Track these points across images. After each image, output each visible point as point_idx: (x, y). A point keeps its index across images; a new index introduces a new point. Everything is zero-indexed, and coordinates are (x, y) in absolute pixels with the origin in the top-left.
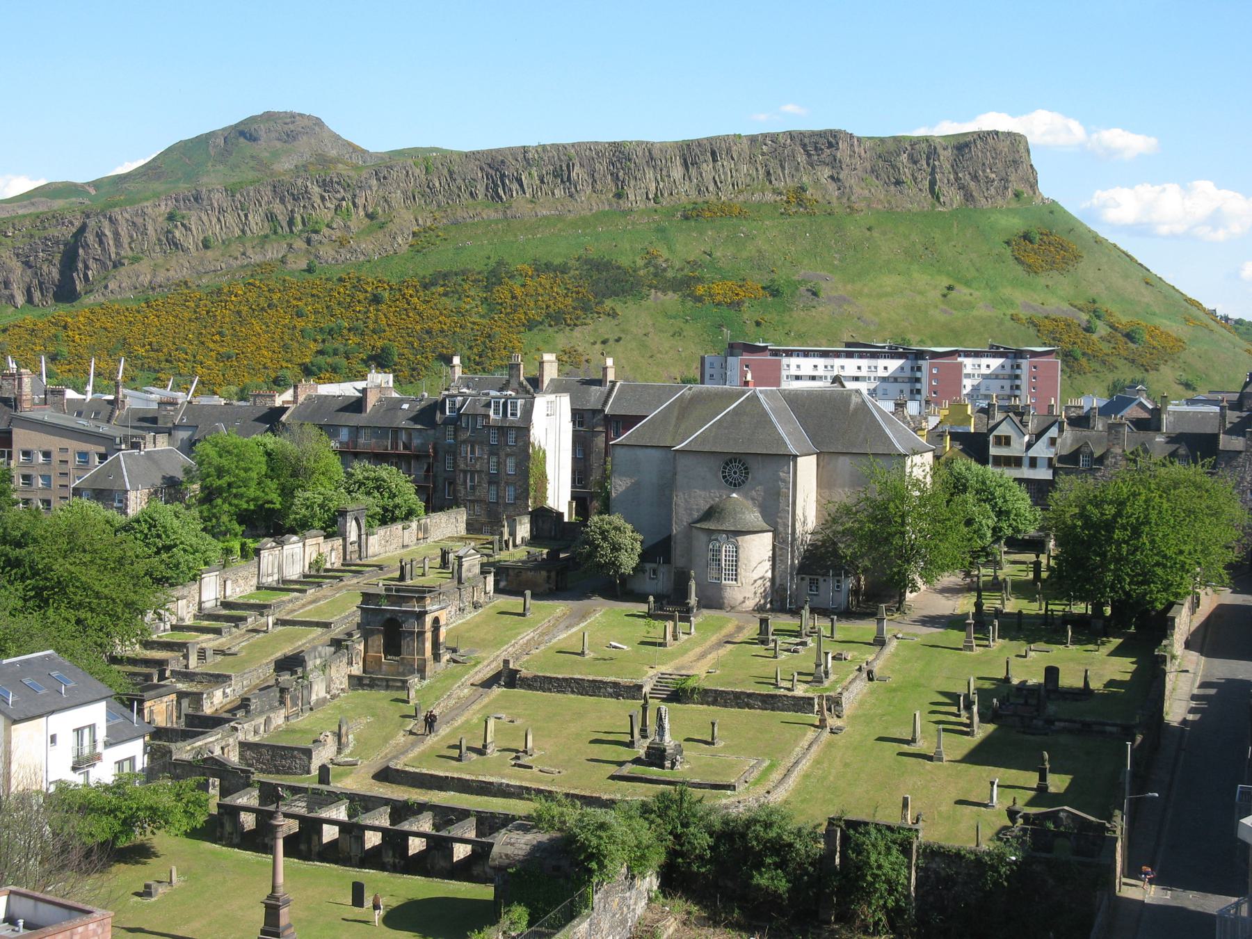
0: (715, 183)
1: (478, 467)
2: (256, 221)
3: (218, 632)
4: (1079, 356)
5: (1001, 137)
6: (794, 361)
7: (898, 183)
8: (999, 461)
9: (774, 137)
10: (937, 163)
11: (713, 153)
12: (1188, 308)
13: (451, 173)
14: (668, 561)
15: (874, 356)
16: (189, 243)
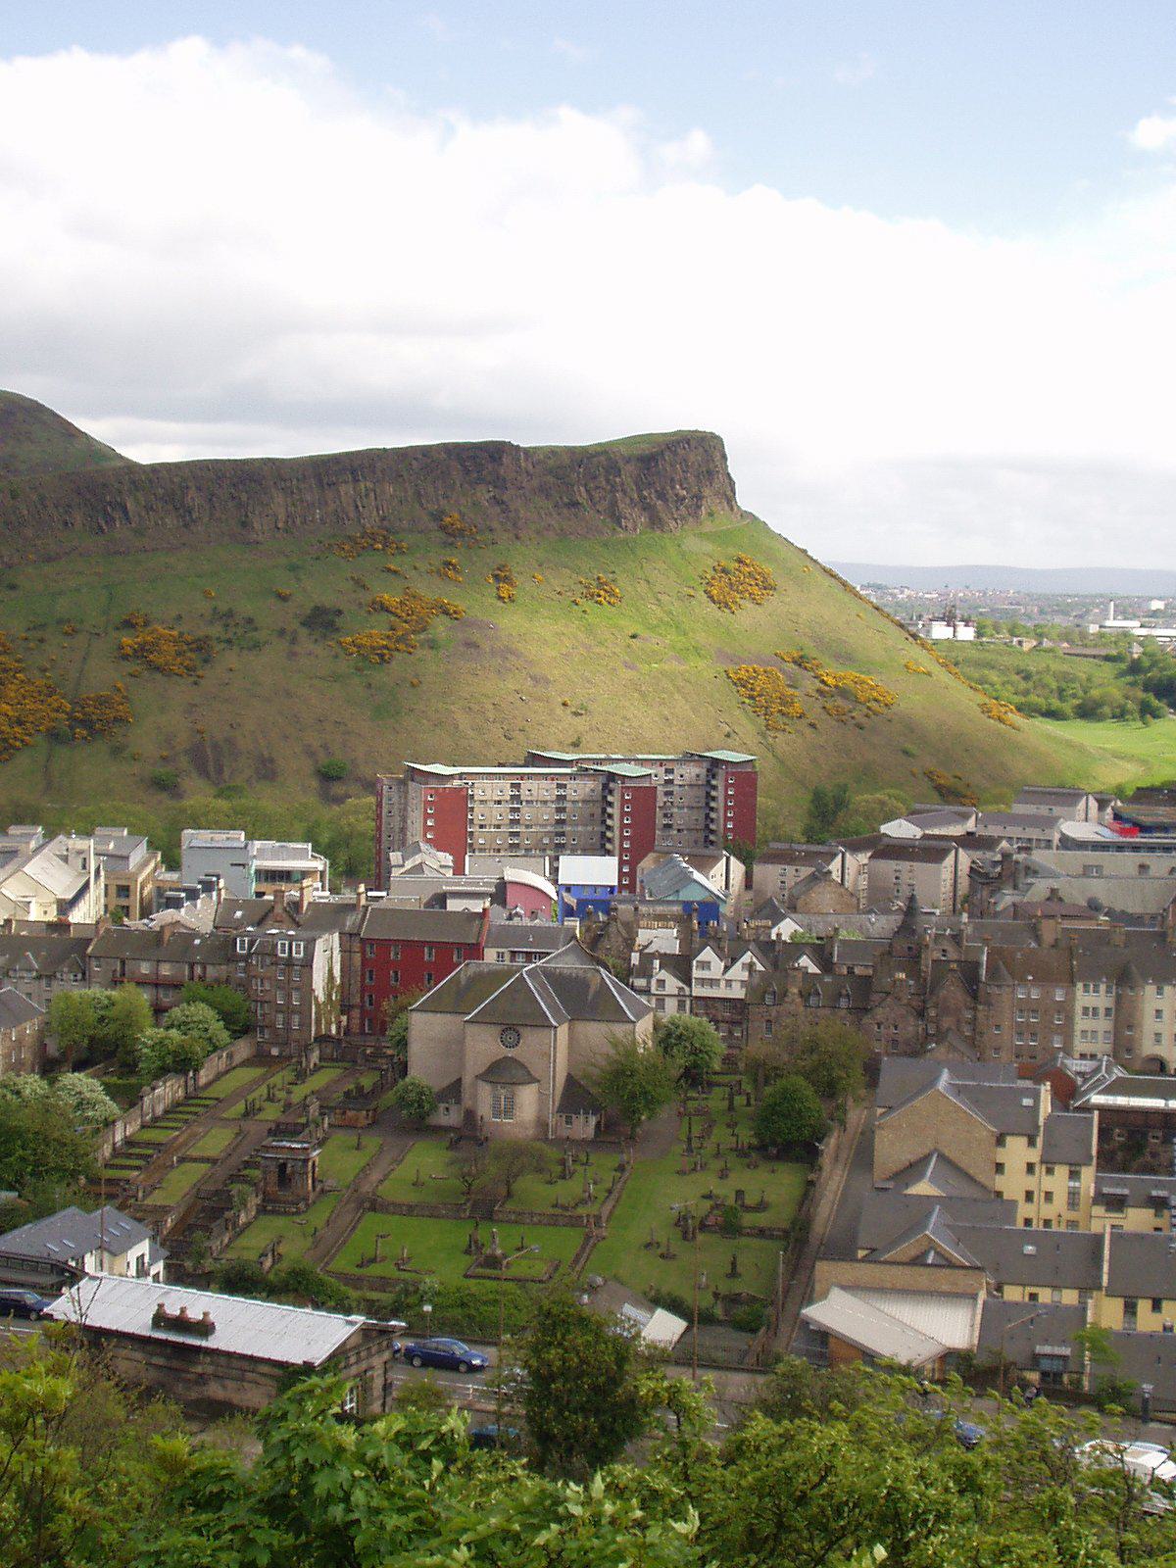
0: (357, 507)
1: (267, 998)
5: (693, 443)
7: (575, 504)
8: (703, 982)
10: (618, 480)
11: (353, 472)
13: (42, 499)
14: (458, 1102)
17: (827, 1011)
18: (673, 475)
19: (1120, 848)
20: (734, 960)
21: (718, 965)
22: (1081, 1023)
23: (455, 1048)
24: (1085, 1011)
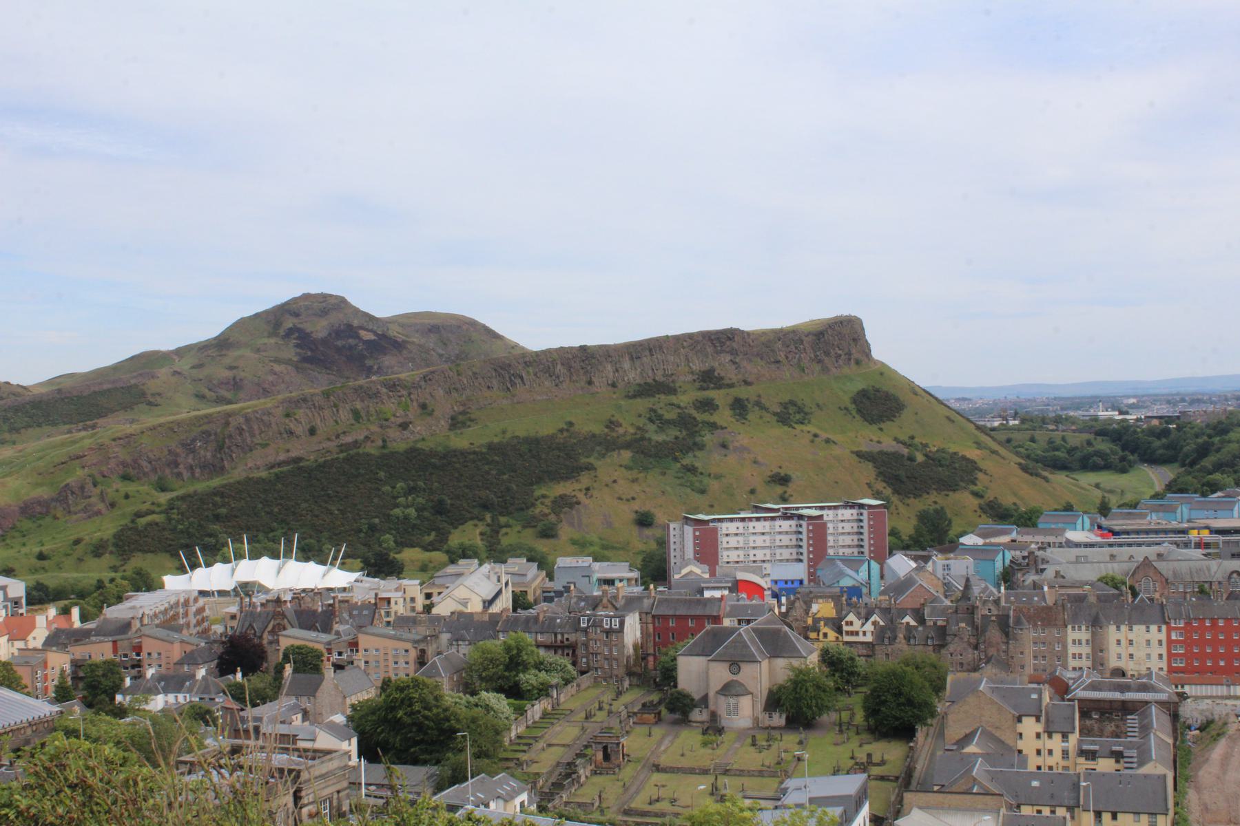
2: (344, 415)
4: (905, 479)
6: (724, 525)
7: (778, 362)
8: (848, 633)
9: (690, 336)
11: (650, 350)
14: (707, 707)
16: (299, 430)
17: (921, 647)
19: (1101, 546)
20: (867, 619)
21: (857, 625)
22: (1072, 649)
24: (1074, 642)
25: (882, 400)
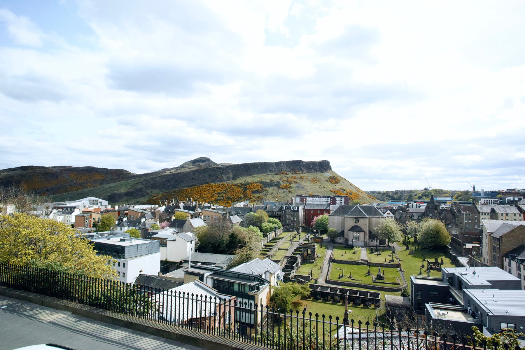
3: (269, 251)
9: (290, 161)
12: (357, 189)
14: (343, 237)
15: (321, 197)
18: (324, 166)
23: (343, 224)
25: (335, 179)
